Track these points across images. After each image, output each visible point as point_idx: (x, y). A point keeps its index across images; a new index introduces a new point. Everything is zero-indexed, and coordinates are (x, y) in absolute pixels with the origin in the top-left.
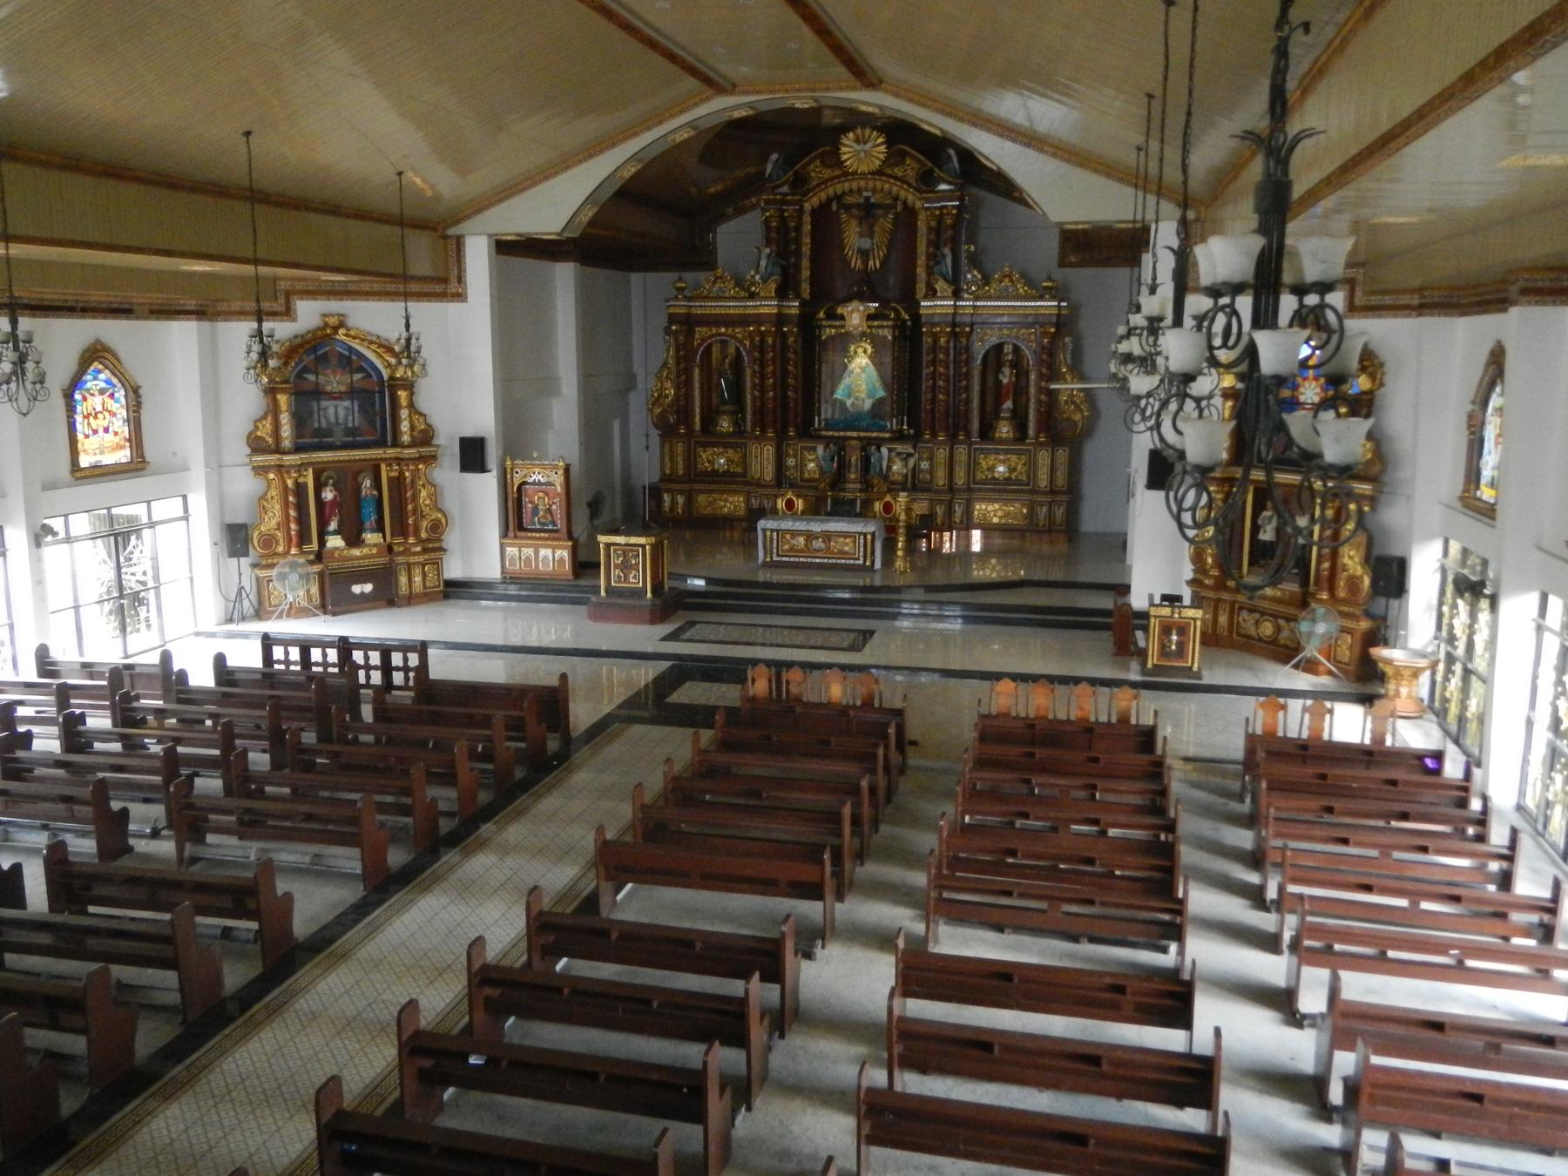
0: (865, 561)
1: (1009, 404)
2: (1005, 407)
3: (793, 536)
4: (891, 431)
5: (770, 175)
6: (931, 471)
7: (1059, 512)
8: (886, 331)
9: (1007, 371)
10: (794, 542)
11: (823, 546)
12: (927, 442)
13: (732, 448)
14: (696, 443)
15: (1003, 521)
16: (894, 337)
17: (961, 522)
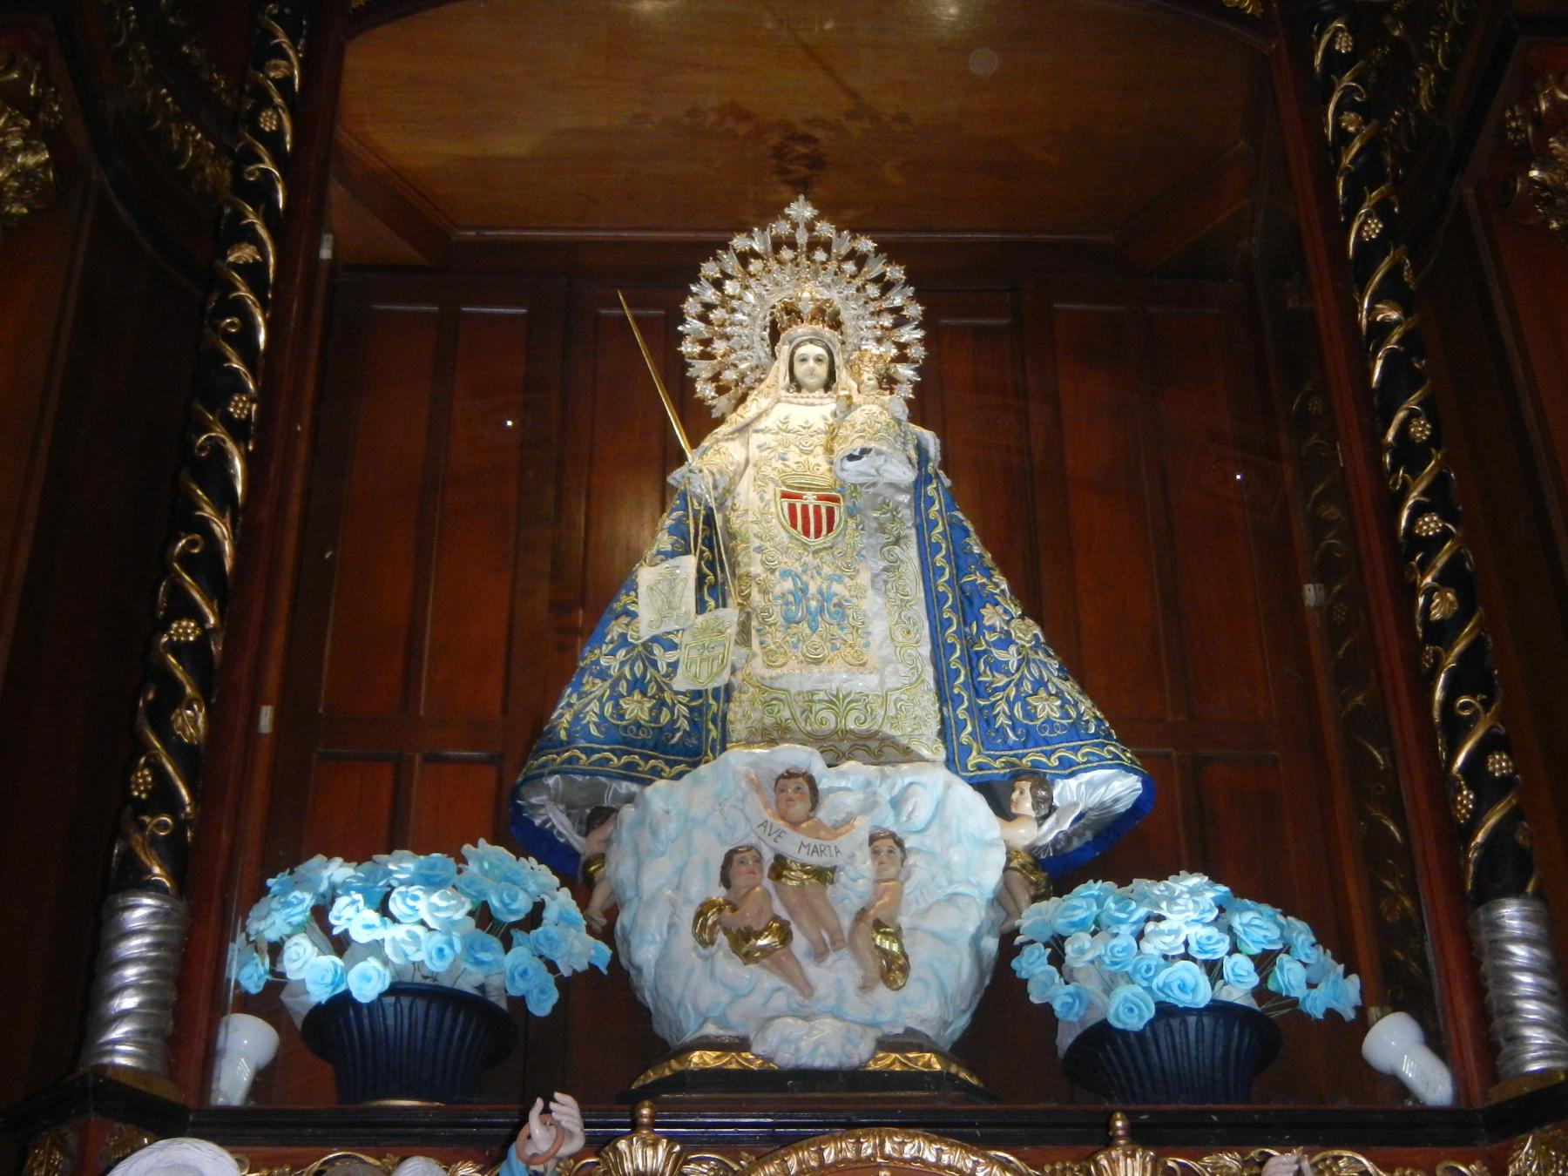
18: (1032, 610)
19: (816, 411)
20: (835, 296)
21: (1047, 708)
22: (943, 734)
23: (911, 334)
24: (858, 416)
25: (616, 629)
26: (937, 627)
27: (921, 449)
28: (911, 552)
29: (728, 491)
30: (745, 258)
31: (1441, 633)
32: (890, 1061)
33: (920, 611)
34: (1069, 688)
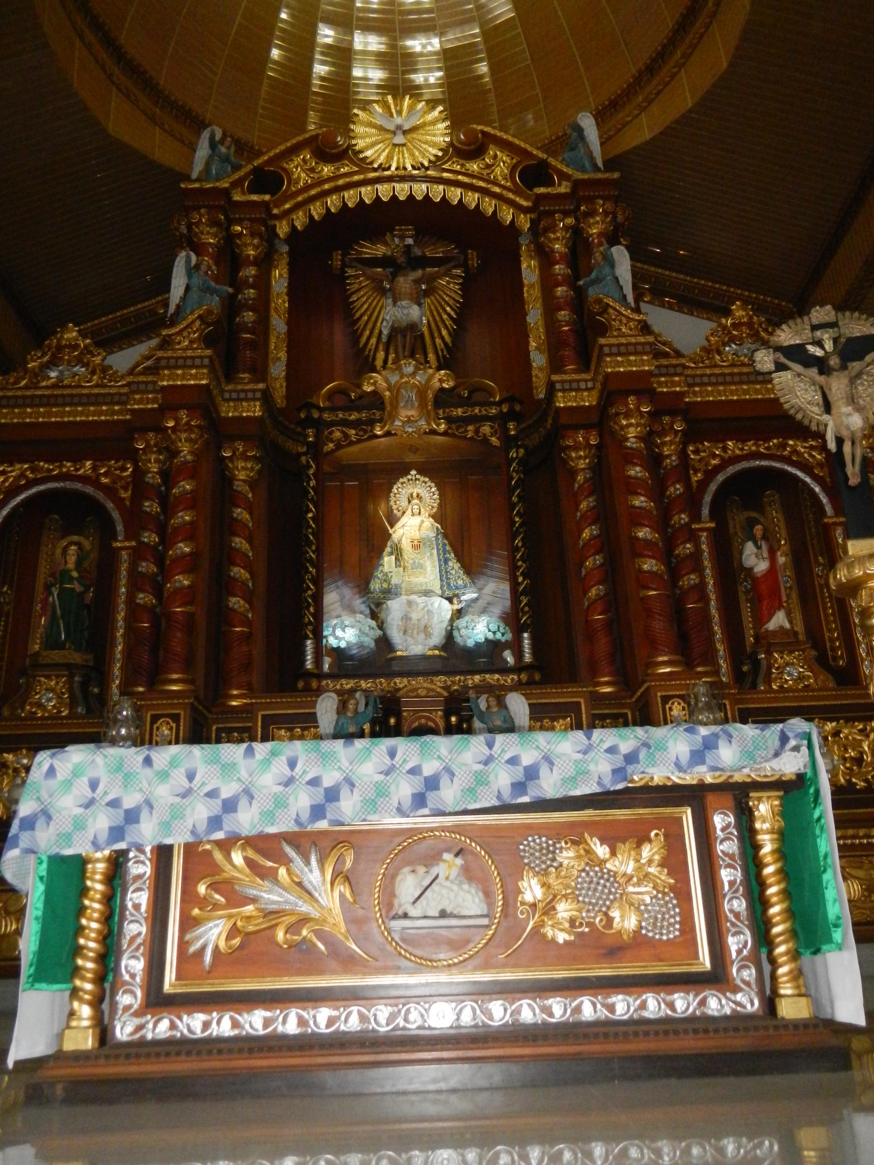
4: (519, 668)
8: (486, 429)
18: (458, 561)
19: (417, 520)
20: (420, 491)
21: (460, 582)
22: (442, 587)
23: (436, 496)
24: (425, 525)
25: (381, 568)
26: (440, 566)
27: (437, 528)
28: (435, 552)
29: (401, 540)
30: (402, 483)
31: (519, 584)
32: (430, 653)
33: (437, 563)
34: (465, 577)
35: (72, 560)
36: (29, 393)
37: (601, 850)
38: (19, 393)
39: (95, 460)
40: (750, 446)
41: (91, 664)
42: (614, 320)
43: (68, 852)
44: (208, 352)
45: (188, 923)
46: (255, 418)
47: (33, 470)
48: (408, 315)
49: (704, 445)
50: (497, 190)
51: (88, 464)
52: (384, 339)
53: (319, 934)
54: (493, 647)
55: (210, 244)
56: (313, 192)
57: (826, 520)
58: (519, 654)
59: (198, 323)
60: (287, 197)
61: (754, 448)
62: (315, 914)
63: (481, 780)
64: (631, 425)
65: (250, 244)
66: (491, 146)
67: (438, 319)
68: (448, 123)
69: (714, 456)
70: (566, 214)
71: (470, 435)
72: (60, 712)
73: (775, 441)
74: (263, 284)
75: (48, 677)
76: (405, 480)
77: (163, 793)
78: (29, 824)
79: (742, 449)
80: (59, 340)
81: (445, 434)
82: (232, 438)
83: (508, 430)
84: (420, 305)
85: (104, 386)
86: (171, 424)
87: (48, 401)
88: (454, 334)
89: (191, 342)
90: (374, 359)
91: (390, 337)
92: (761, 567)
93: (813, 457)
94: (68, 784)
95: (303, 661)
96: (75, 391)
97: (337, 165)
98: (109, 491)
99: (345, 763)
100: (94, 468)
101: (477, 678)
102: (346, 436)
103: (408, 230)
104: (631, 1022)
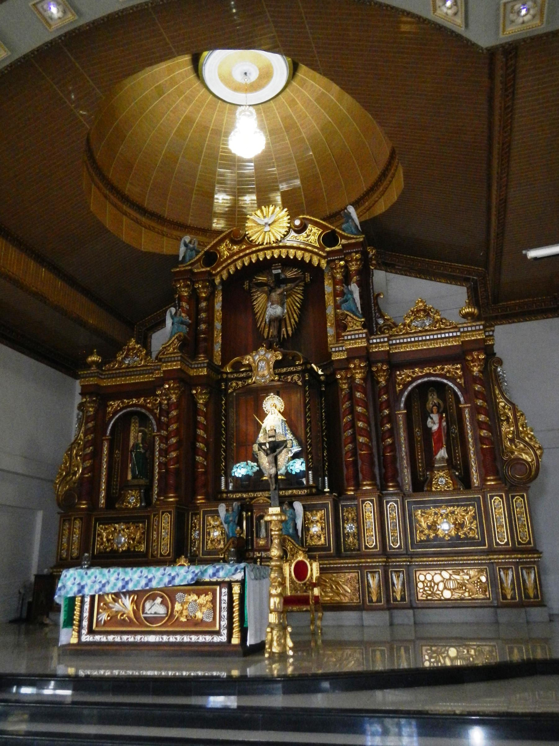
0: (230, 636)
1: (443, 453)
2: (438, 457)
3: (117, 596)
4: (308, 487)
5: (184, 257)
6: (359, 535)
7: (530, 579)
8: (296, 377)
9: (435, 417)
10: (117, 607)
11: (161, 610)
12: (352, 498)
13: (133, 523)
14: (97, 520)
15: (456, 596)
16: (304, 381)
17: (403, 599)
19: (274, 416)
31: (308, 449)
35: (140, 439)
36: (118, 371)
37: (195, 597)
38: (114, 372)
39: (145, 397)
40: (426, 370)
41: (148, 484)
42: (350, 322)
43: (69, 596)
44: (180, 354)
45: (98, 613)
46: (204, 375)
47: (123, 403)
48: (275, 312)
49: (403, 371)
50: (310, 248)
51: (142, 399)
52: (267, 323)
53: (128, 617)
54: (304, 474)
55: (185, 296)
56: (229, 261)
57: (460, 406)
58: (308, 481)
59: (176, 340)
60: (218, 266)
61: (428, 371)
62: (126, 611)
63: (161, 580)
64: (357, 373)
65: (203, 292)
66: (309, 225)
67: (292, 309)
68: (289, 217)
69: (408, 376)
70: (341, 260)
71: (289, 380)
72: (137, 505)
73: (439, 367)
74: (210, 309)
75: (132, 490)
76: (269, 397)
77: (89, 582)
78: (60, 589)
79: (421, 372)
80: (128, 347)
81: (279, 380)
82: (195, 386)
83: (304, 377)
84: (282, 305)
85: (147, 366)
86: (167, 386)
87: (126, 375)
88: (300, 317)
89: (174, 349)
90: (264, 332)
91: (270, 321)
92: (435, 428)
93: (457, 373)
94: (69, 579)
95: (220, 486)
96: (134, 369)
97: (240, 245)
98: (151, 411)
99: (130, 574)
100: (145, 400)
101: (290, 491)
102: (237, 384)
103: (278, 266)
104: (195, 642)
